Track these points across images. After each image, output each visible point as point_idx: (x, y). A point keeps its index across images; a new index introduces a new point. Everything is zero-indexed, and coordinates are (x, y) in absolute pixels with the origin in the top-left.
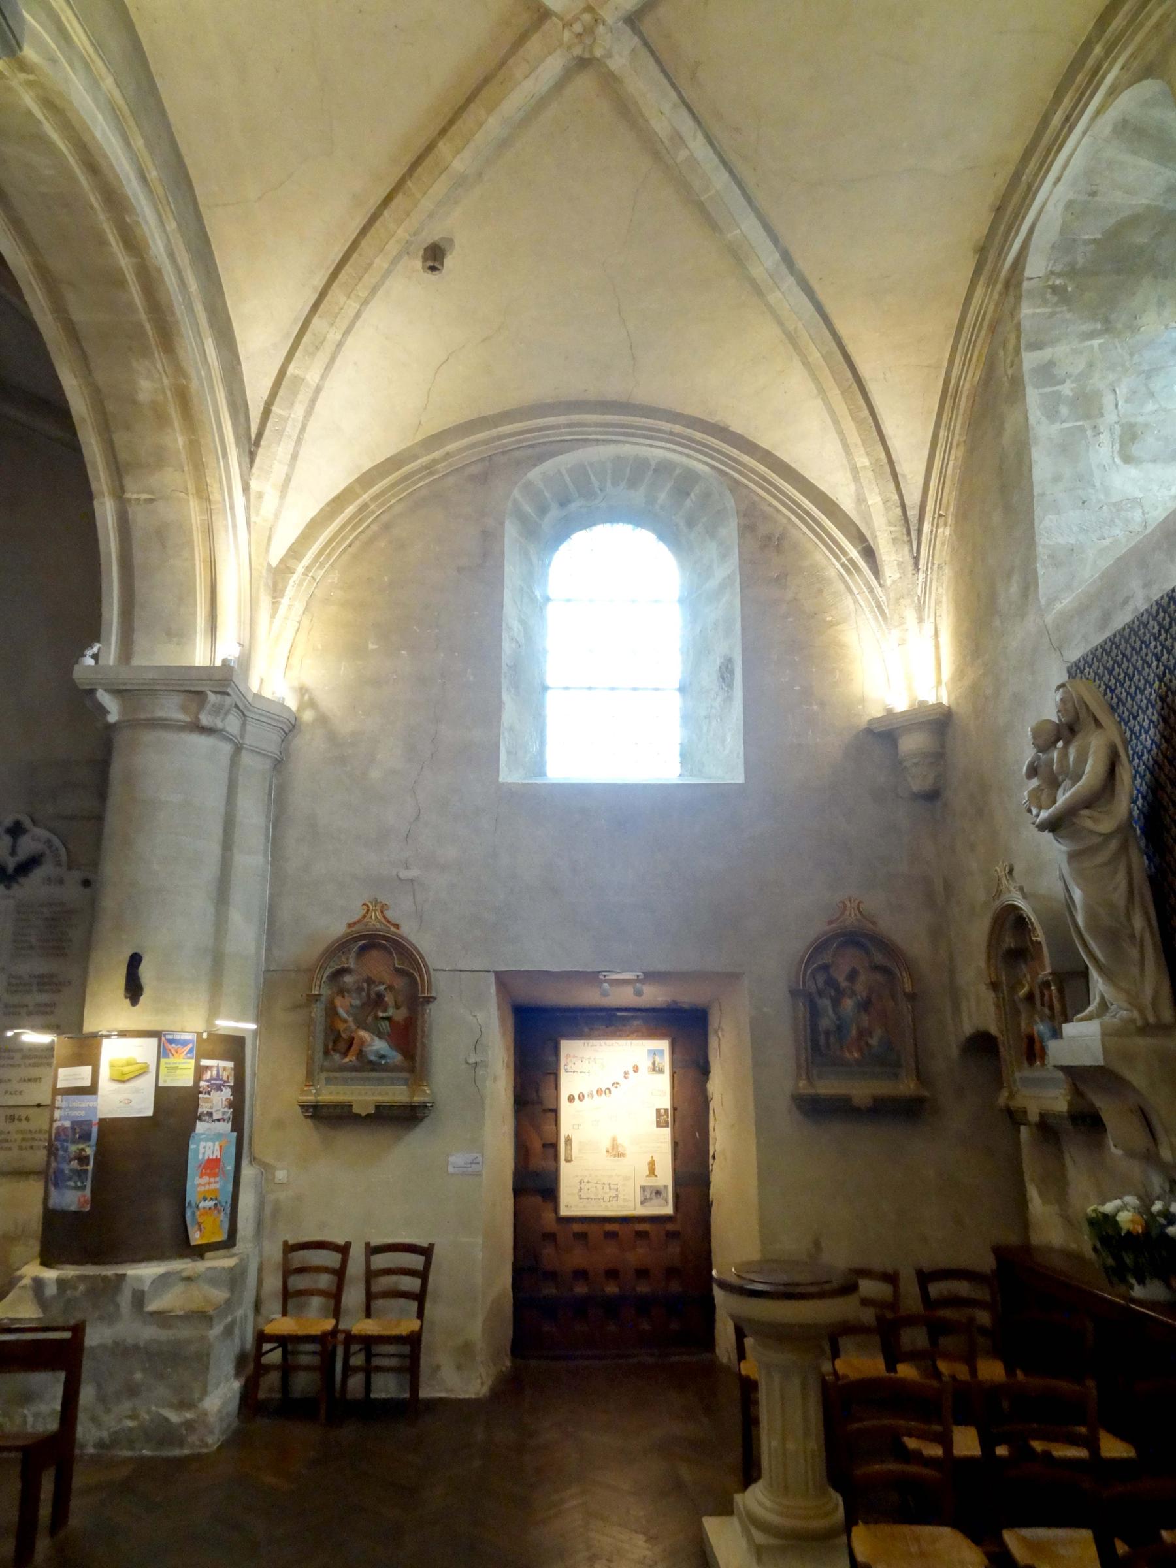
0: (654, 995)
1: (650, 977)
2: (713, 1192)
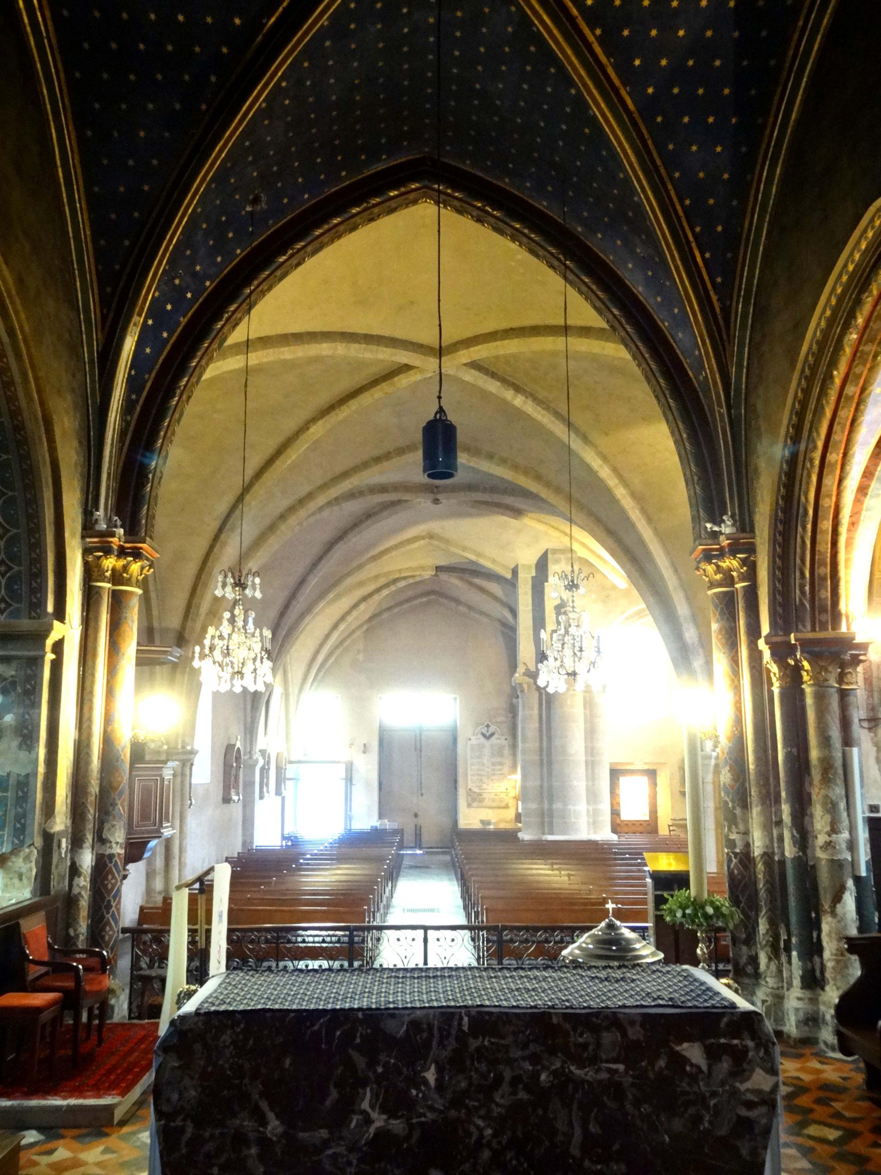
0: (646, 767)
1: (646, 763)
2: (659, 814)
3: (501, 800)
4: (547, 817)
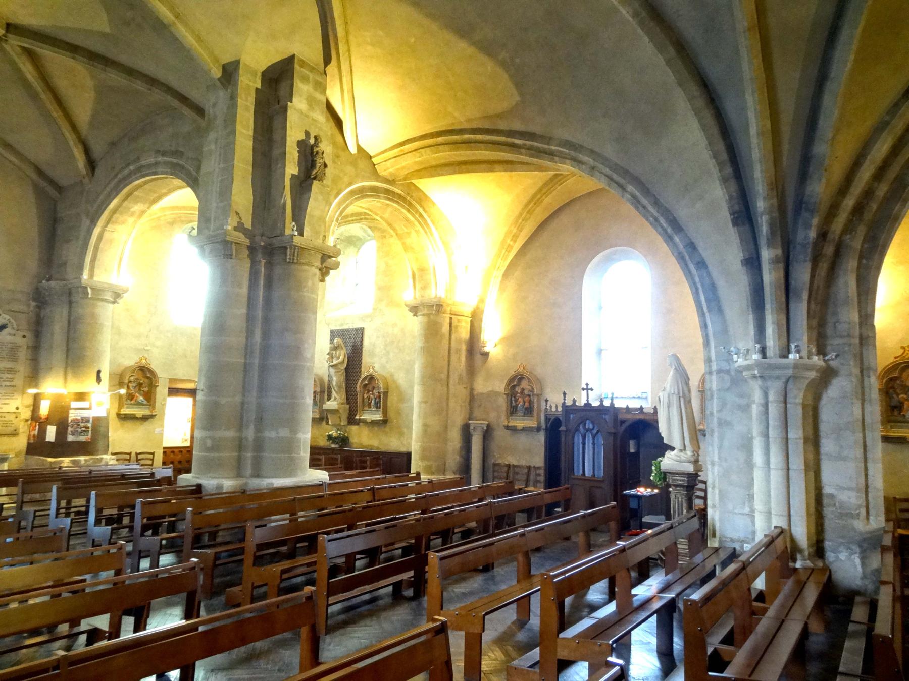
3: (6, 424)
4: (250, 452)
